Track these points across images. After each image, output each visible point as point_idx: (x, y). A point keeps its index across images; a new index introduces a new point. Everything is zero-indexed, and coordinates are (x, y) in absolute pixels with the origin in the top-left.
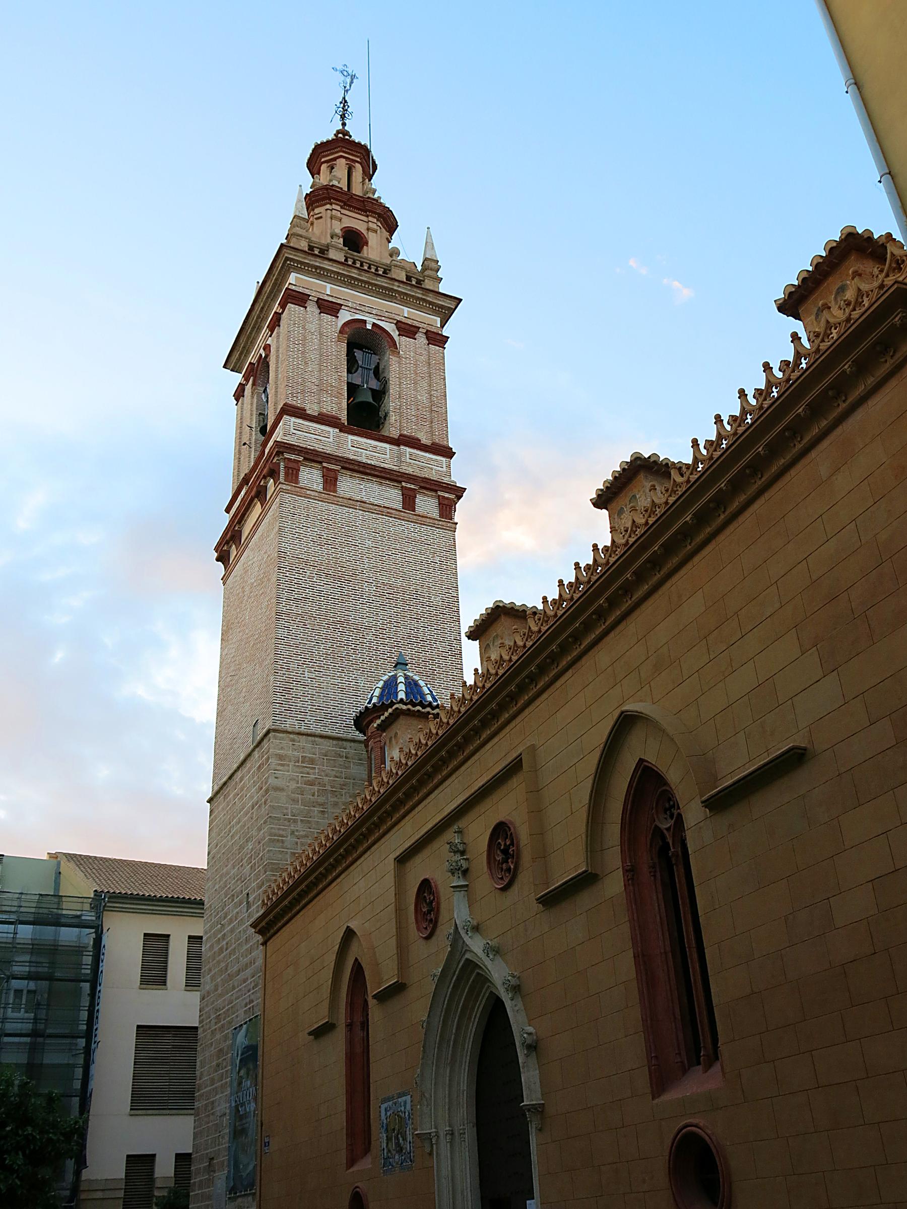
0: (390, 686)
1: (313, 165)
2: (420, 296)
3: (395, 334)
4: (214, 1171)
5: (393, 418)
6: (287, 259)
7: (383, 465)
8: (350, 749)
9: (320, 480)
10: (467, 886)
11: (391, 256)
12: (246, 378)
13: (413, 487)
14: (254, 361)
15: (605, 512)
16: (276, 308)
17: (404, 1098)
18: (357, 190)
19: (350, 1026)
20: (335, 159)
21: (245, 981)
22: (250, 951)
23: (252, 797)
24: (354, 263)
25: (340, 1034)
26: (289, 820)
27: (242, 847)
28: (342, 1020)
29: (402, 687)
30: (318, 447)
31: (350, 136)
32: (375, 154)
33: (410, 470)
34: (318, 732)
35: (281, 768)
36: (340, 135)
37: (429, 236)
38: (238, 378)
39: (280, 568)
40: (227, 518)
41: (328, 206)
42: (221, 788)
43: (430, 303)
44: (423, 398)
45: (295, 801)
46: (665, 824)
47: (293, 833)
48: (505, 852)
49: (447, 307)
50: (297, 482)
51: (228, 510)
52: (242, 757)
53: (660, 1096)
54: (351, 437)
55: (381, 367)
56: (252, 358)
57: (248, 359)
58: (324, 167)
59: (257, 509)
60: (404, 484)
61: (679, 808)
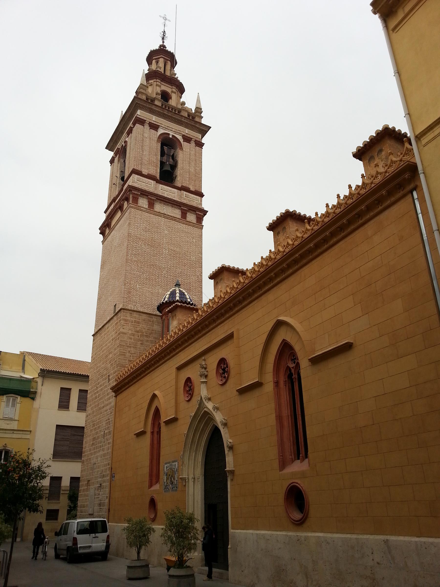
0: (173, 294)
1: (149, 59)
2: (193, 124)
3: (181, 140)
4: (90, 486)
6: (137, 103)
7: (174, 199)
8: (154, 319)
10: (207, 382)
11: (182, 105)
12: (116, 154)
13: (186, 209)
14: (120, 147)
15: (272, 233)
16: (131, 125)
17: (175, 463)
18: (168, 73)
19: (152, 433)
20: (159, 58)
21: (106, 411)
22: (109, 399)
23: (112, 336)
24: (166, 107)
26: (128, 346)
27: (107, 356)
28: (149, 429)
29: (178, 295)
31: (166, 48)
32: (177, 57)
33: (185, 202)
34: (142, 310)
35: (125, 325)
36: (162, 47)
37: (198, 97)
38: (111, 154)
39: (128, 240)
41: (155, 80)
42: (99, 331)
43: (197, 128)
44: (192, 170)
46: (291, 365)
47: (129, 352)
48: (224, 370)
50: (137, 204)
52: (108, 319)
53: (282, 470)
54: (161, 185)
55: (175, 155)
56: (119, 146)
59: (119, 214)
60: (182, 207)
61: (298, 359)
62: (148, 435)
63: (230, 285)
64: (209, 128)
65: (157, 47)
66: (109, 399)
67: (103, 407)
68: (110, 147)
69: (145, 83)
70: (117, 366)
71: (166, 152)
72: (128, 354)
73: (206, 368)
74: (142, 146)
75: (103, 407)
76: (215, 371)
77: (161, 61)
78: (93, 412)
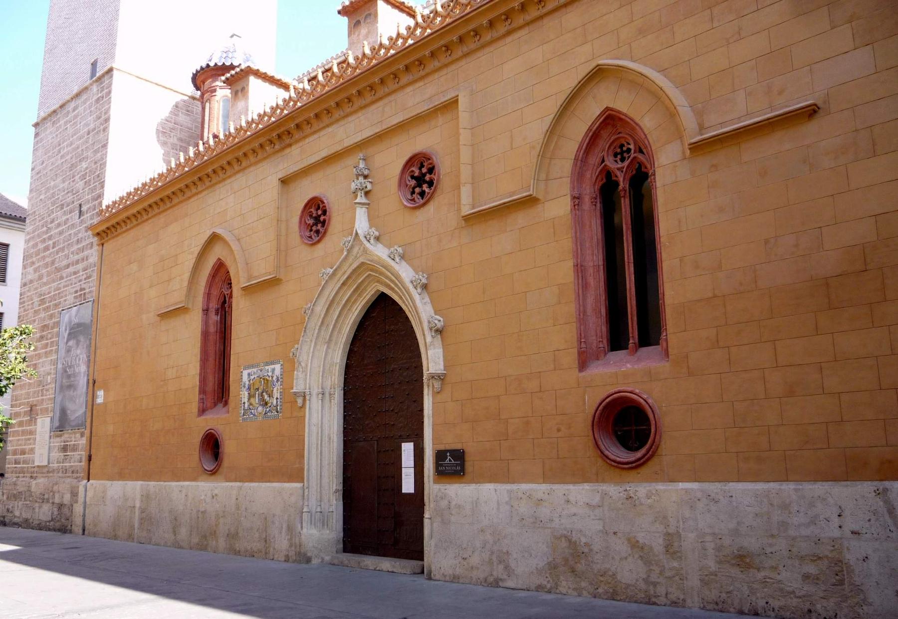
10: (368, 204)
17: (273, 366)
23: (87, 125)
27: (73, 166)
67: (68, 266)
75: (68, 266)
78: (40, 278)
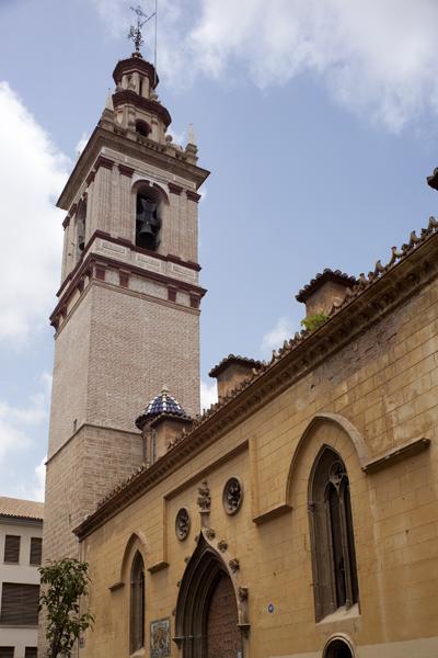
0: (158, 402)
1: (117, 76)
3: (167, 191)
5: (163, 245)
8: (131, 439)
9: (118, 279)
12: (71, 213)
16: (92, 169)
18: (145, 95)
19: (133, 586)
25: (128, 588)
28: (128, 582)
30: (117, 258)
32: (159, 71)
33: (173, 277)
38: (64, 214)
39: (92, 331)
40: (55, 301)
45: (99, 465)
49: (201, 176)
51: (58, 295)
56: (75, 201)
57: (72, 201)
58: (124, 78)
59: (78, 295)
62: (128, 588)
63: (237, 380)
64: (209, 173)
65: (129, 56)
66: (71, 545)
68: (62, 202)
69: (112, 108)
70: (81, 502)
71: (145, 207)
72: (95, 487)
73: (207, 495)
74: (110, 199)
76: (221, 498)
77: (135, 75)
